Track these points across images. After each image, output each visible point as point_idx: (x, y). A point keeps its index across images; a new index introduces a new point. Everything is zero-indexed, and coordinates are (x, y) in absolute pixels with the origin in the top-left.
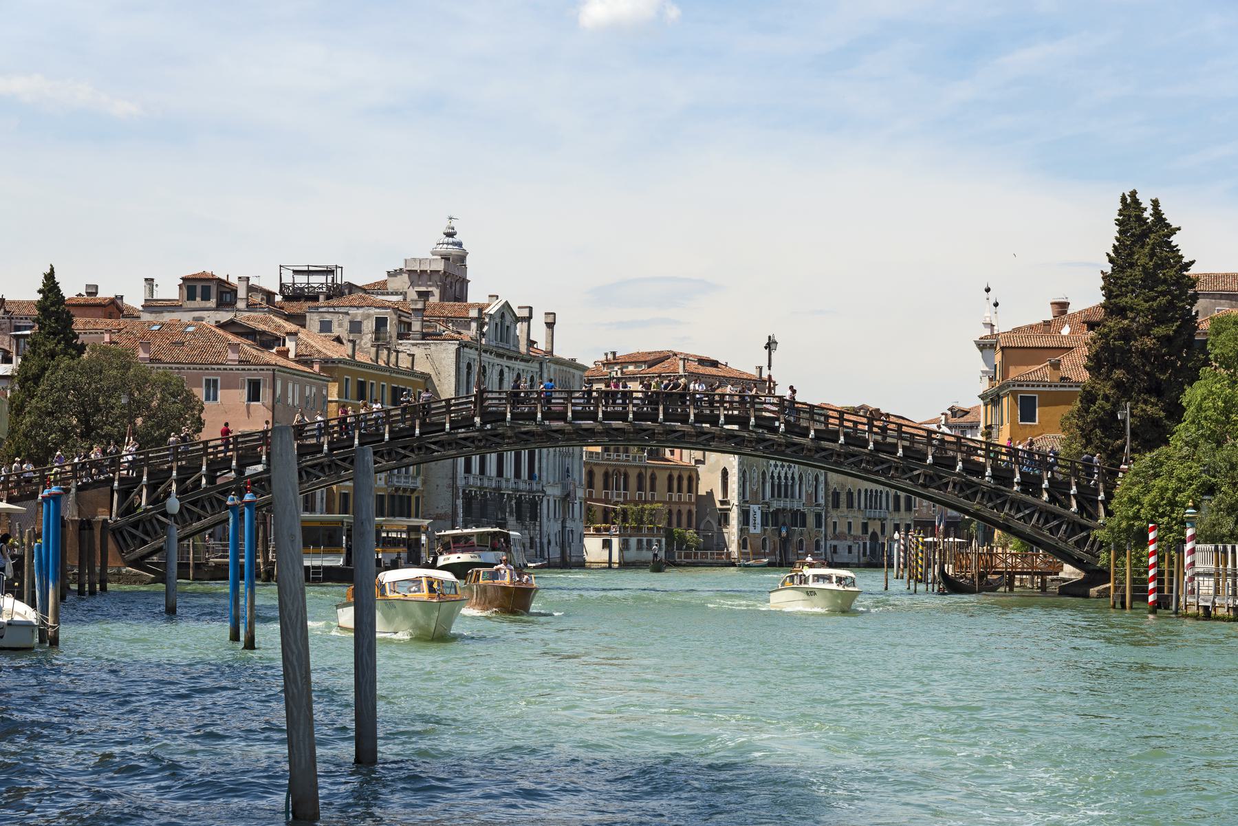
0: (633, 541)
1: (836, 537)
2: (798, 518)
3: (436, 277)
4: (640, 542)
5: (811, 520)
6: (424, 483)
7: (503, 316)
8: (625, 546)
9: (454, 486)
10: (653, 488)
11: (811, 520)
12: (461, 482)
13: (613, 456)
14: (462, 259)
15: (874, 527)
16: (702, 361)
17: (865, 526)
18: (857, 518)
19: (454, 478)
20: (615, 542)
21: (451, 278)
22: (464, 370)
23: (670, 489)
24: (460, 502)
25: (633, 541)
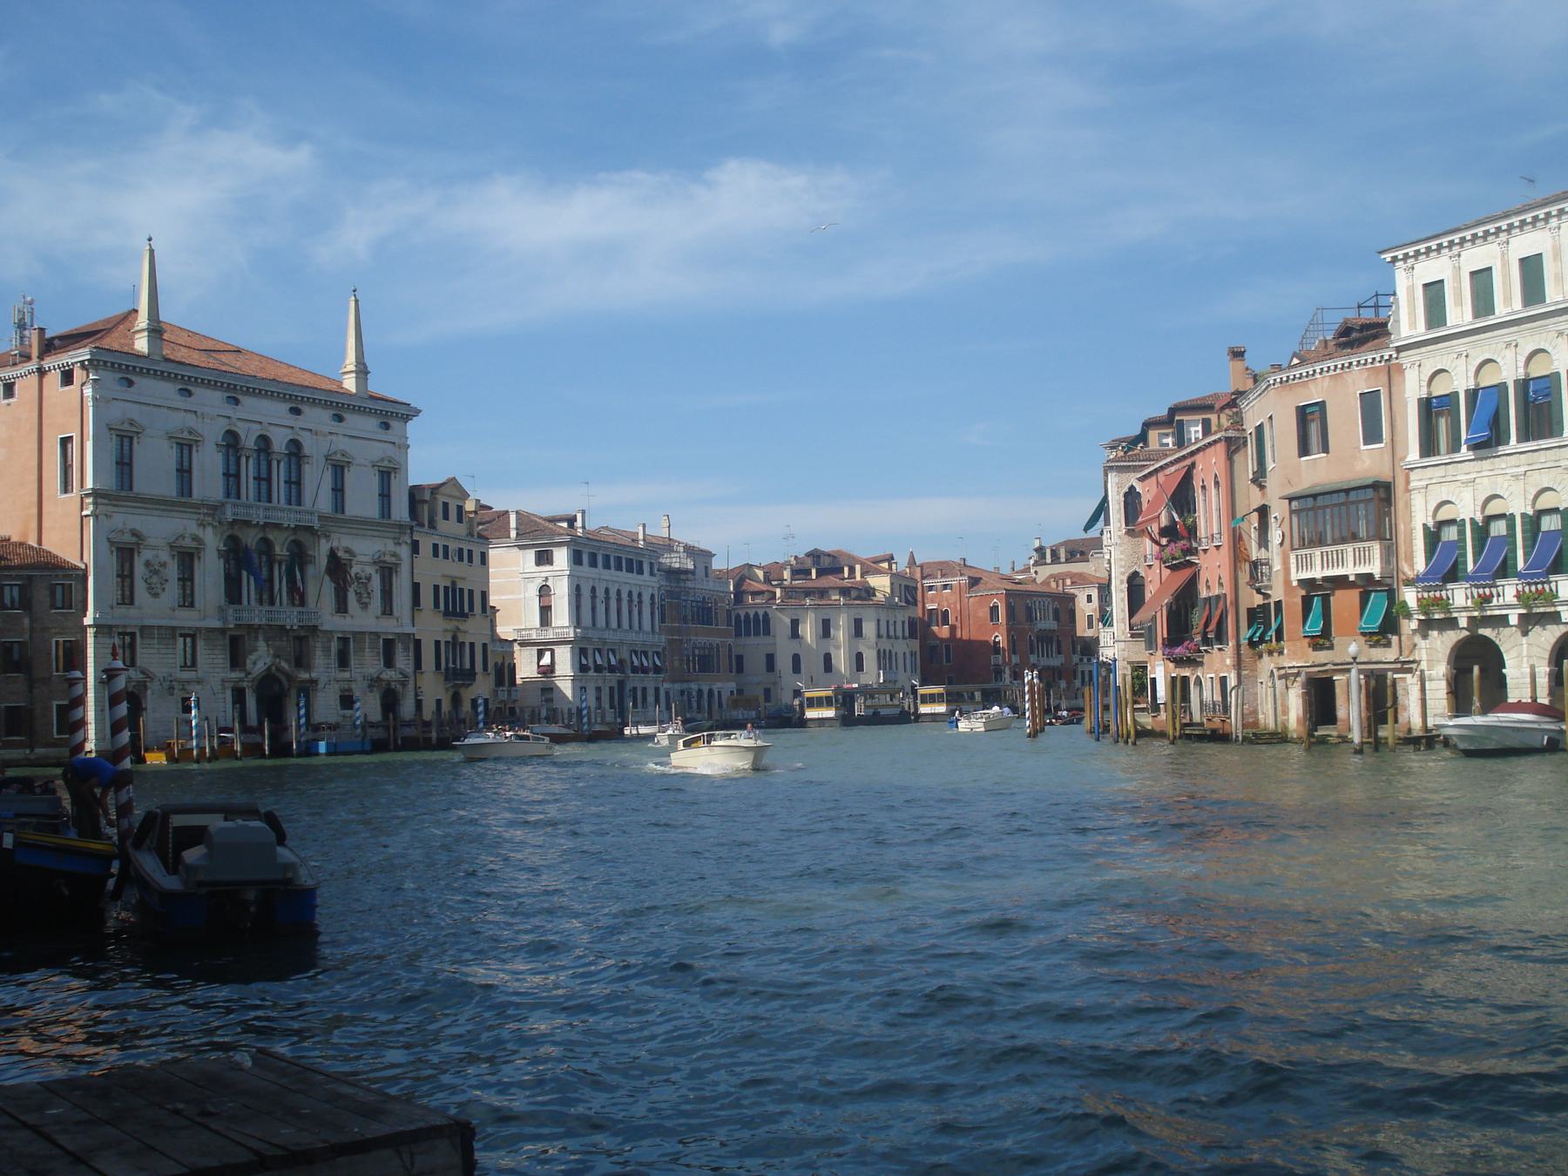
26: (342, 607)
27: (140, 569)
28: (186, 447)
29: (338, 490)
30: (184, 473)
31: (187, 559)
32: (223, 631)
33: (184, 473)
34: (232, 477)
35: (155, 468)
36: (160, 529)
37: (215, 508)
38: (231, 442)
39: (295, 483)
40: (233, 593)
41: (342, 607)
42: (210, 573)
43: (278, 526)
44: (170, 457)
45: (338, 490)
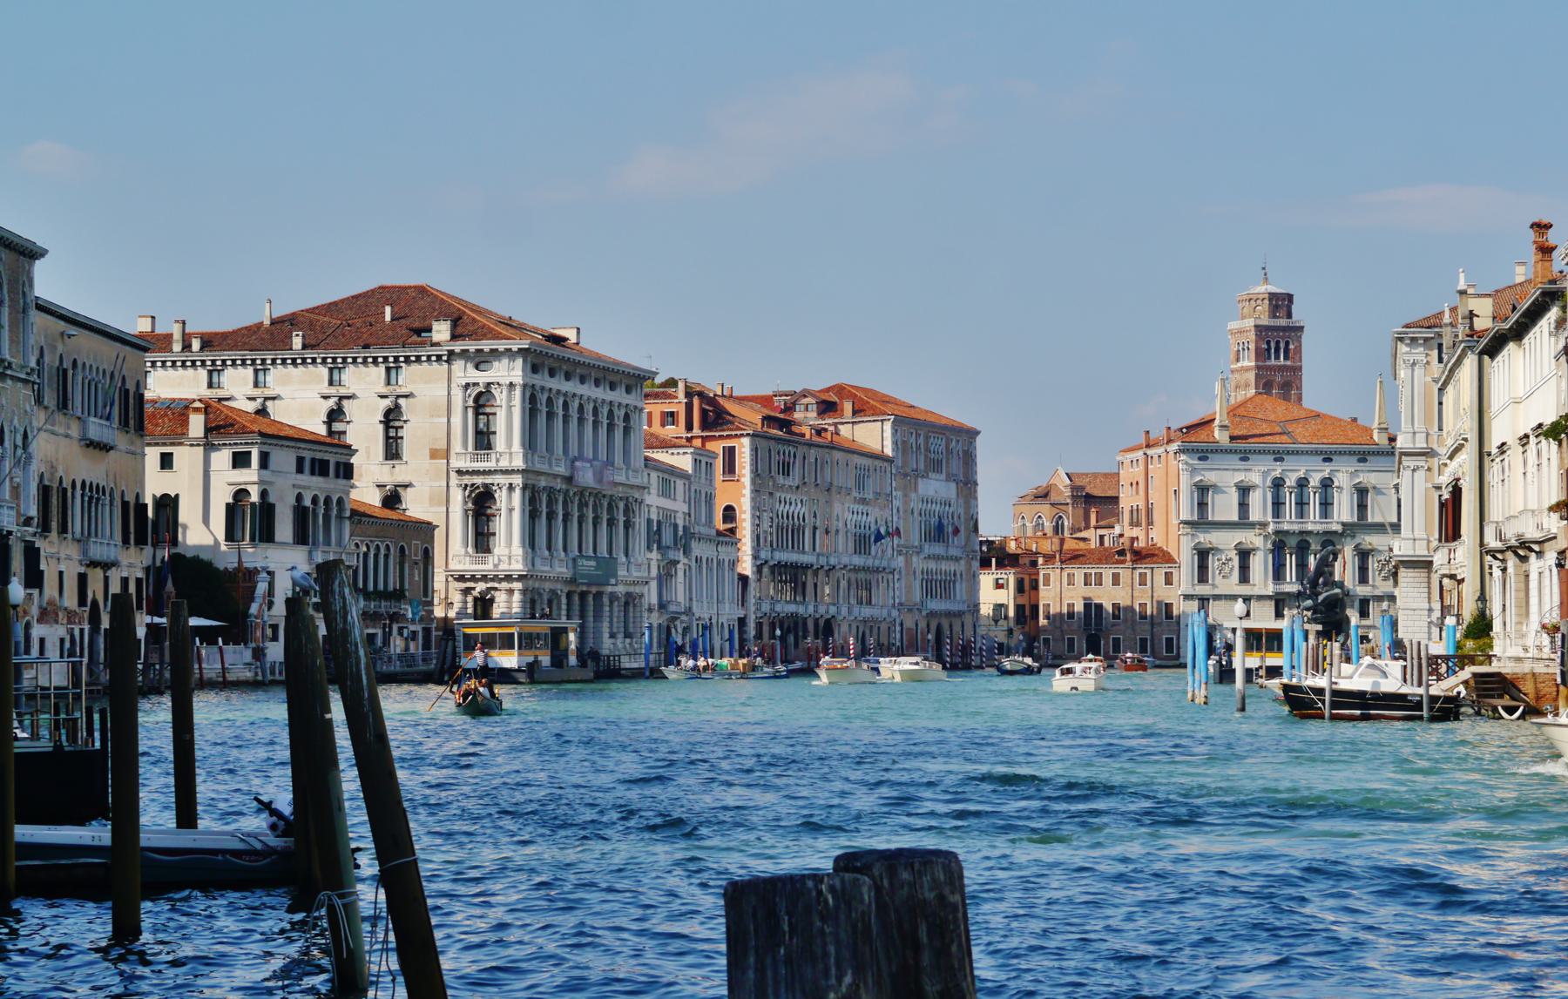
26: (1363, 580)
27: (1213, 563)
28: (1244, 491)
29: (1362, 507)
30: (1243, 506)
31: (1244, 554)
32: (1269, 597)
33: (1243, 506)
34: (1278, 505)
35: (1224, 507)
36: (1226, 541)
37: (1264, 525)
38: (1278, 484)
39: (1326, 505)
40: (1278, 575)
41: (1363, 580)
42: (1259, 565)
43: (1310, 533)
44: (1234, 496)
45: (1362, 507)
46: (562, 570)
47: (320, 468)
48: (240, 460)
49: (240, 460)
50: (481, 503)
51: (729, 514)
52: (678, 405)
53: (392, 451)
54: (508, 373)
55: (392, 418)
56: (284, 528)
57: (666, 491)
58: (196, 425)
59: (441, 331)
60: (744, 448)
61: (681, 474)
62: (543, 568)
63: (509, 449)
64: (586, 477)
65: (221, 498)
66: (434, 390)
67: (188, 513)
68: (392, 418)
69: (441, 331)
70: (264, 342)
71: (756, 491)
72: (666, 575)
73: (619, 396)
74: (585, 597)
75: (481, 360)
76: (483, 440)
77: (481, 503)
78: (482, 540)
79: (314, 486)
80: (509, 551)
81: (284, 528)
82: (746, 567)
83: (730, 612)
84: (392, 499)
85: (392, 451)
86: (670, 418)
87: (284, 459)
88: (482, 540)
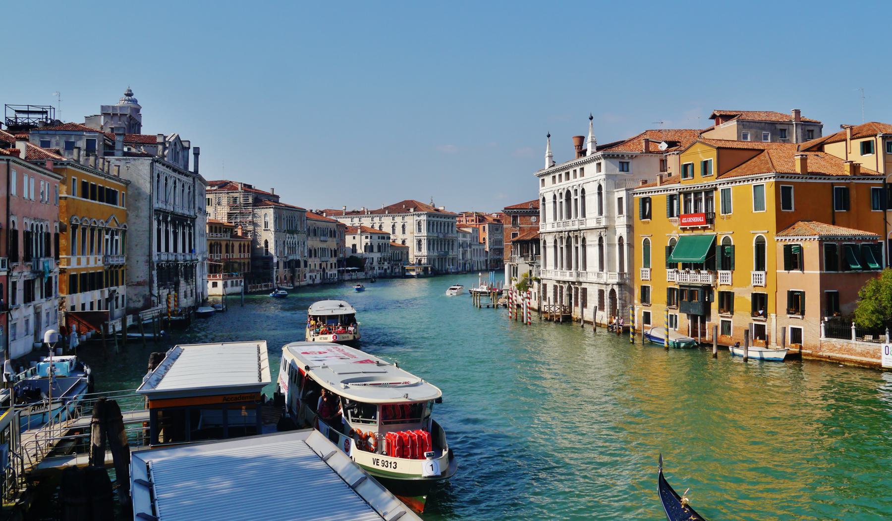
0: (229, 282)
1: (311, 271)
2: (298, 263)
3: (124, 119)
4: (232, 282)
5: (302, 264)
6: (127, 259)
7: (175, 144)
8: (225, 286)
9: (150, 262)
10: (233, 252)
11: (302, 264)
12: (155, 258)
13: (214, 235)
14: (137, 110)
15: (324, 265)
16: (245, 185)
17: (321, 265)
18: (317, 261)
19: (150, 255)
20: (220, 283)
21: (130, 120)
22: (156, 179)
23: (240, 252)
24: (155, 273)
25: (229, 282)
46: (436, 254)
47: (383, 238)
48: (367, 238)
49: (367, 238)
50: (419, 242)
51: (484, 239)
52: (474, 218)
53: (404, 232)
54: (424, 218)
55: (403, 226)
56: (375, 249)
57: (464, 236)
58: (359, 231)
59: (412, 210)
60: (487, 226)
61: (469, 233)
62: (431, 254)
63: (424, 232)
64: (441, 236)
65: (363, 244)
66: (411, 221)
67: (358, 247)
68: (403, 226)
69: (412, 210)
70: (381, 212)
71: (489, 234)
72: (464, 254)
73: (450, 220)
74: (443, 258)
75: (419, 215)
76: (420, 230)
77: (419, 242)
78: (420, 249)
79: (382, 241)
80: (424, 251)
81: (375, 249)
82: (487, 249)
83: (483, 259)
84: (404, 242)
85: (404, 232)
86: (473, 221)
87: (375, 237)
88: (420, 249)
